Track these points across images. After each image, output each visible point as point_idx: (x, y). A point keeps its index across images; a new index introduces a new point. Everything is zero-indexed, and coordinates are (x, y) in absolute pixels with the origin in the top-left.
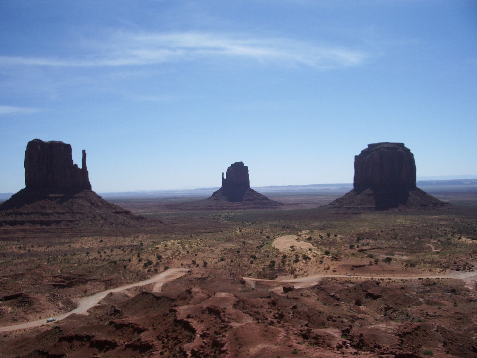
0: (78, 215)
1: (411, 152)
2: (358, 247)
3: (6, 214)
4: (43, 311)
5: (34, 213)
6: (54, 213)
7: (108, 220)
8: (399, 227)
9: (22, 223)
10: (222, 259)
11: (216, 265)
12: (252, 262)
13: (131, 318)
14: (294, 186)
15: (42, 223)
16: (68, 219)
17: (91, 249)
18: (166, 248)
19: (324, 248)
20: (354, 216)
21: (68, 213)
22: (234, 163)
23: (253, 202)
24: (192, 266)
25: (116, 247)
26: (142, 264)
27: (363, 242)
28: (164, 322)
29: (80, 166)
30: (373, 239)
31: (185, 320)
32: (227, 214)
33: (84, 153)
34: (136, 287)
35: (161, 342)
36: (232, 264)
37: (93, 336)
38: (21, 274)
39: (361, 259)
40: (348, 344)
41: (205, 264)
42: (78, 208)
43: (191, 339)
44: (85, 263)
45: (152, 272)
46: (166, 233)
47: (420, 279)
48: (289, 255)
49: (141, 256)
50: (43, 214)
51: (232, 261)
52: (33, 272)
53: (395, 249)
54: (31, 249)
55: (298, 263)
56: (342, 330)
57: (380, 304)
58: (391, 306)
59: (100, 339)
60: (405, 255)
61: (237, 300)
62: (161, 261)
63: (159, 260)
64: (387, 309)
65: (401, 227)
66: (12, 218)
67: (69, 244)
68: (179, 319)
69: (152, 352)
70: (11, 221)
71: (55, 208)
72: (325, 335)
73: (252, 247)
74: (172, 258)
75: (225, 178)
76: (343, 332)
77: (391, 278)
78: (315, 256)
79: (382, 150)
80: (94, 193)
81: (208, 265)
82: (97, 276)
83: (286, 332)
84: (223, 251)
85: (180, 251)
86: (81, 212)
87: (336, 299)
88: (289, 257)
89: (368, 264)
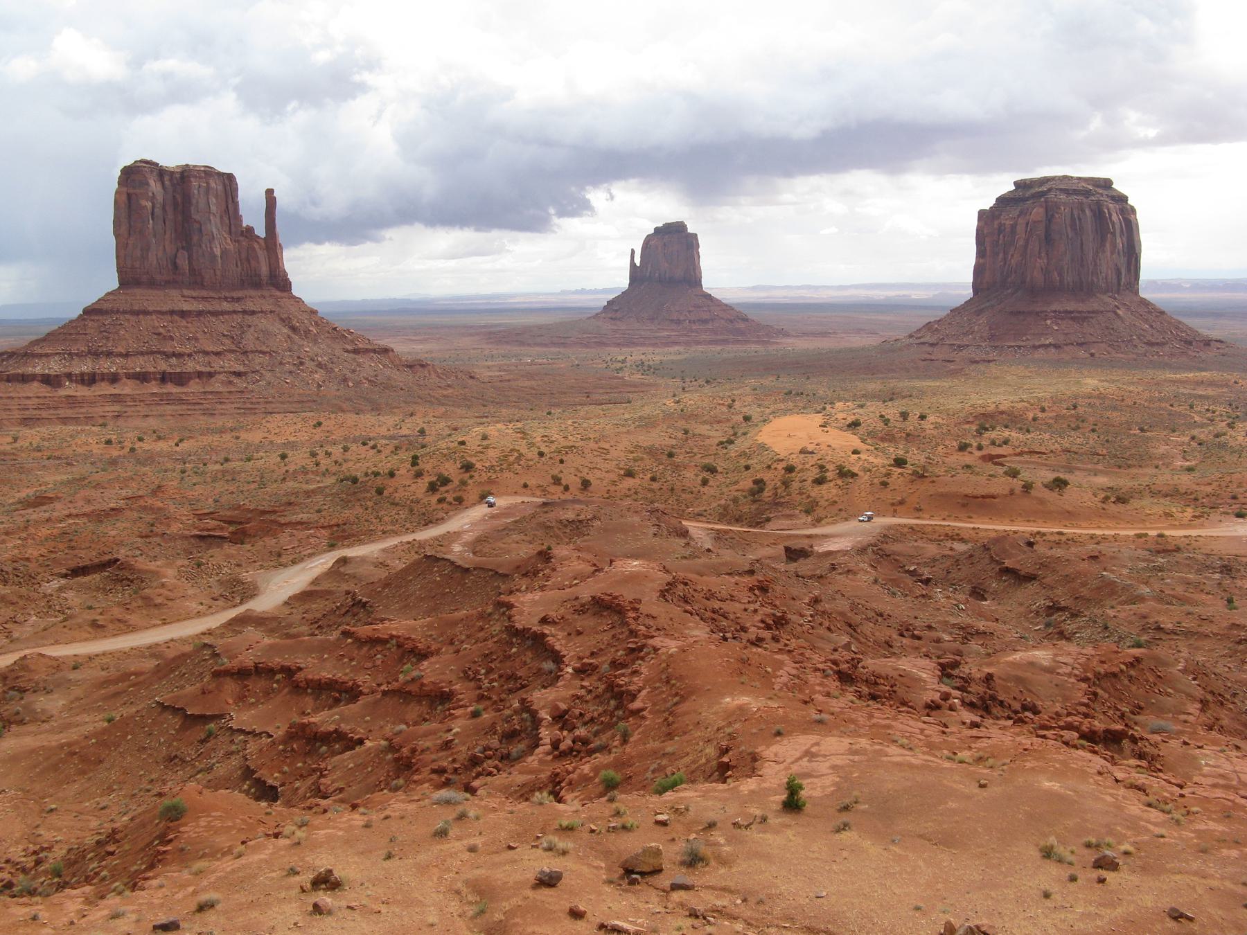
0: (258, 359)
2: (980, 448)
4: (170, 603)
5: (142, 354)
6: (195, 352)
7: (337, 370)
8: (1089, 401)
9: (114, 379)
10: (630, 474)
11: (612, 488)
12: (705, 482)
13: (399, 625)
14: (816, 288)
15: (164, 378)
16: (232, 370)
17: (292, 445)
18: (485, 443)
19: (892, 450)
20: (973, 366)
21: (232, 351)
22: (660, 225)
24: (552, 489)
25: (355, 441)
26: (423, 484)
27: (993, 435)
28: (481, 634)
29: (261, 231)
30: (1021, 429)
31: (535, 628)
32: (643, 357)
34: (409, 543)
35: (472, 684)
36: (655, 485)
37: (300, 669)
38: (113, 509)
39: (989, 480)
40: (956, 701)
41: (586, 484)
42: (258, 339)
43: (552, 679)
44: (276, 481)
45: (451, 504)
46: (484, 406)
47: (1139, 536)
48: (800, 467)
49: (422, 466)
50: (168, 356)
51: (653, 479)
52: (142, 502)
53: (1076, 456)
54: (138, 445)
55: (824, 486)
56: (940, 664)
57: (1032, 596)
58: (1063, 604)
59: (317, 677)
60: (1106, 474)
61: (669, 578)
62: (471, 477)
63: (468, 475)
64: (1054, 608)
65: (1092, 401)
67: (233, 434)
68: (519, 626)
69: (449, 709)
70: (82, 374)
71: (197, 339)
72: (895, 674)
73: (707, 442)
74: (501, 470)
75: (638, 264)
76: (943, 667)
77: (1065, 531)
78: (869, 470)
80: (298, 300)
81: (591, 488)
82: (309, 513)
83: (797, 665)
84: (632, 452)
85: (522, 451)
86: (264, 348)
87: (921, 581)
88: (802, 470)
89: (1006, 492)
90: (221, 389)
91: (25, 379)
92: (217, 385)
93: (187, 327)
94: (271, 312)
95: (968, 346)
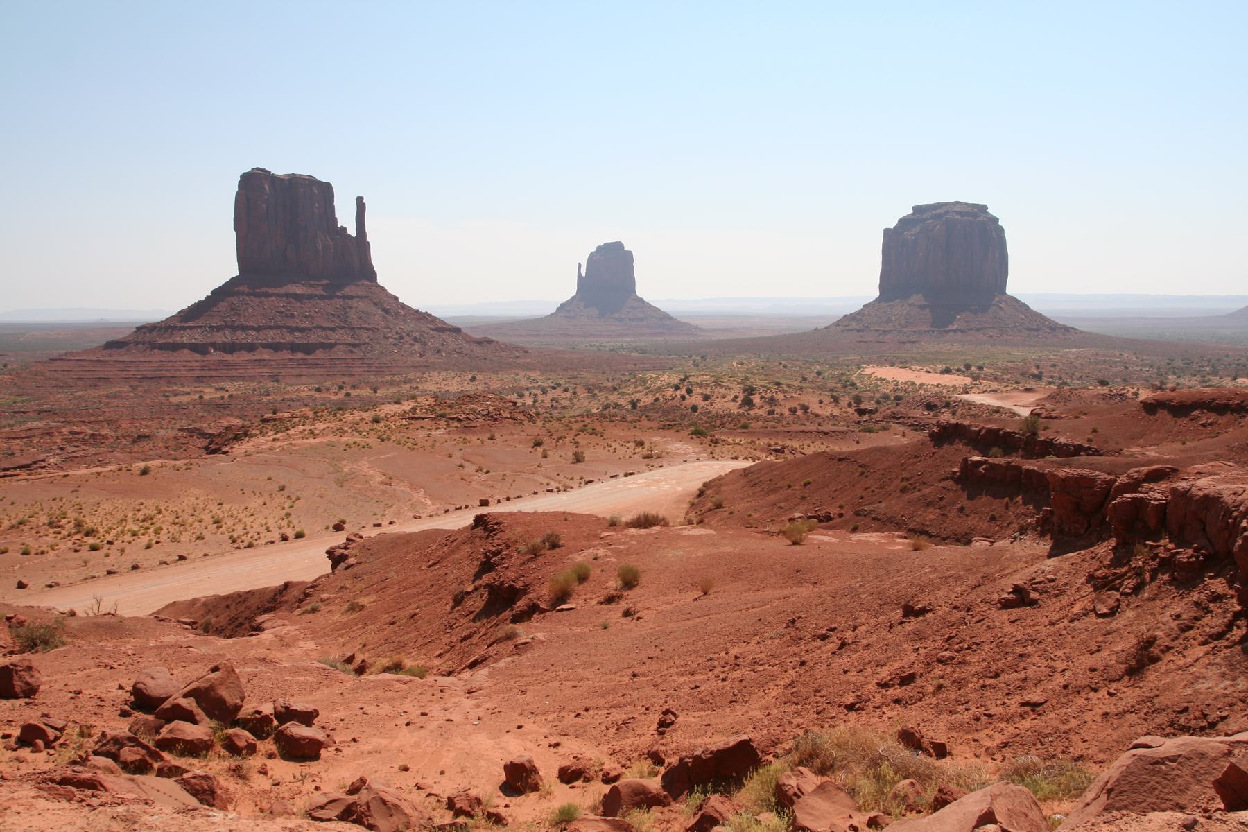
0: (365, 334)
3: (211, 327)
5: (271, 328)
7: (429, 343)
9: (251, 348)
15: (294, 348)
21: (343, 328)
23: (645, 323)
29: (352, 231)
33: (361, 204)
42: (360, 318)
50: (292, 330)
66: (227, 338)
70: (224, 343)
75: (584, 275)
79: (949, 216)
86: (367, 326)
90: (344, 357)
91: (176, 347)
92: (339, 352)
93: (301, 307)
94: (366, 297)
95: (891, 331)
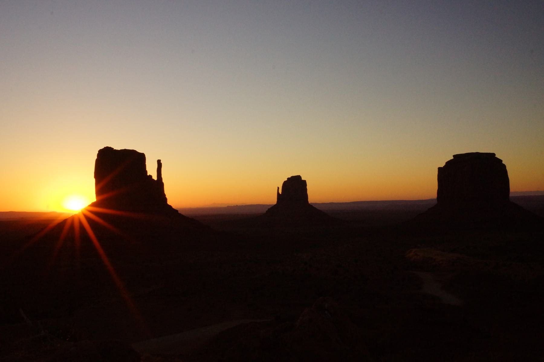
1: (503, 162)
29: (155, 177)
33: (159, 163)
75: (280, 193)
